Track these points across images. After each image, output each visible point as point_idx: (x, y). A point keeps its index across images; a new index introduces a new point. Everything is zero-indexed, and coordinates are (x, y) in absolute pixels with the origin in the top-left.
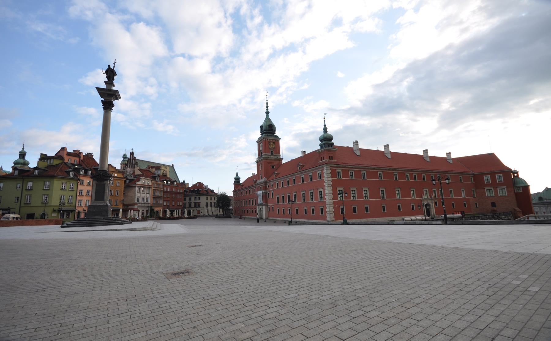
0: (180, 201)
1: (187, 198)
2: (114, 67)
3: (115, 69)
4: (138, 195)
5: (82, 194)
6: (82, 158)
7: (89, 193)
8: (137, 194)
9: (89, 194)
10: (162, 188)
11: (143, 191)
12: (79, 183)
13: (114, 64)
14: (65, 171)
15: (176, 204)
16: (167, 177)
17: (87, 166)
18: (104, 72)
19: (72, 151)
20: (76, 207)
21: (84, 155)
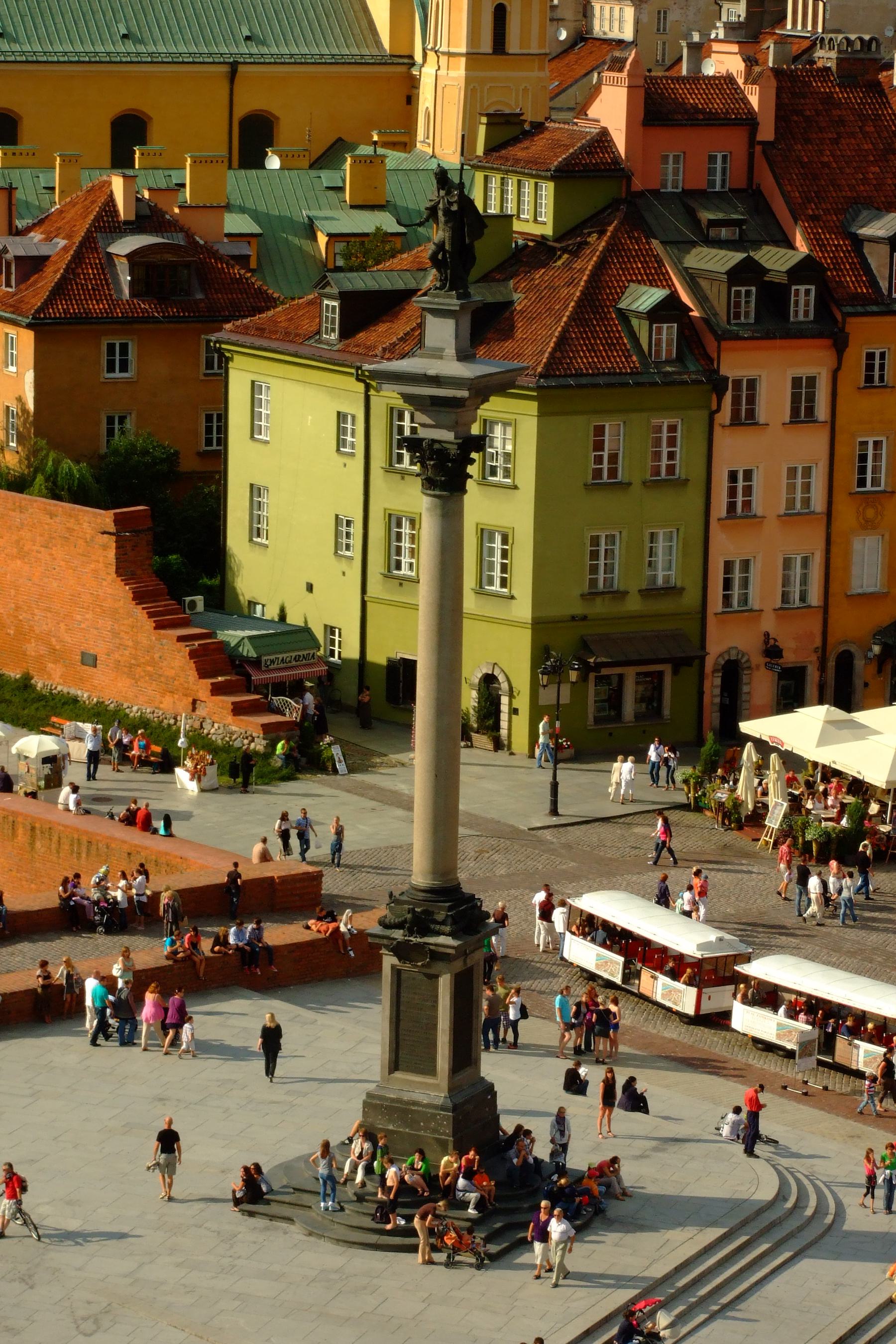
5: (747, 504)
6: (767, 132)
7: (807, 487)
9: (806, 502)
12: (725, 415)
20: (711, 621)
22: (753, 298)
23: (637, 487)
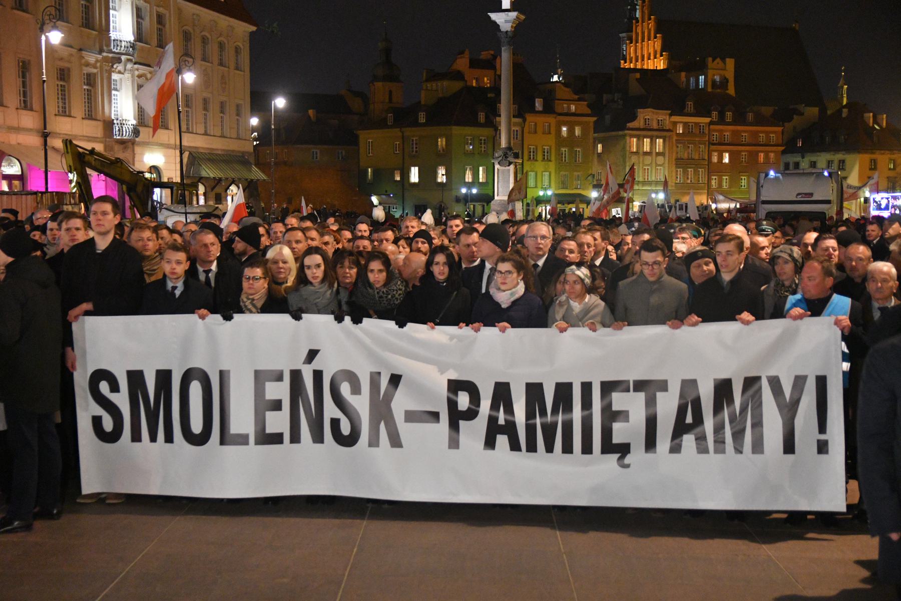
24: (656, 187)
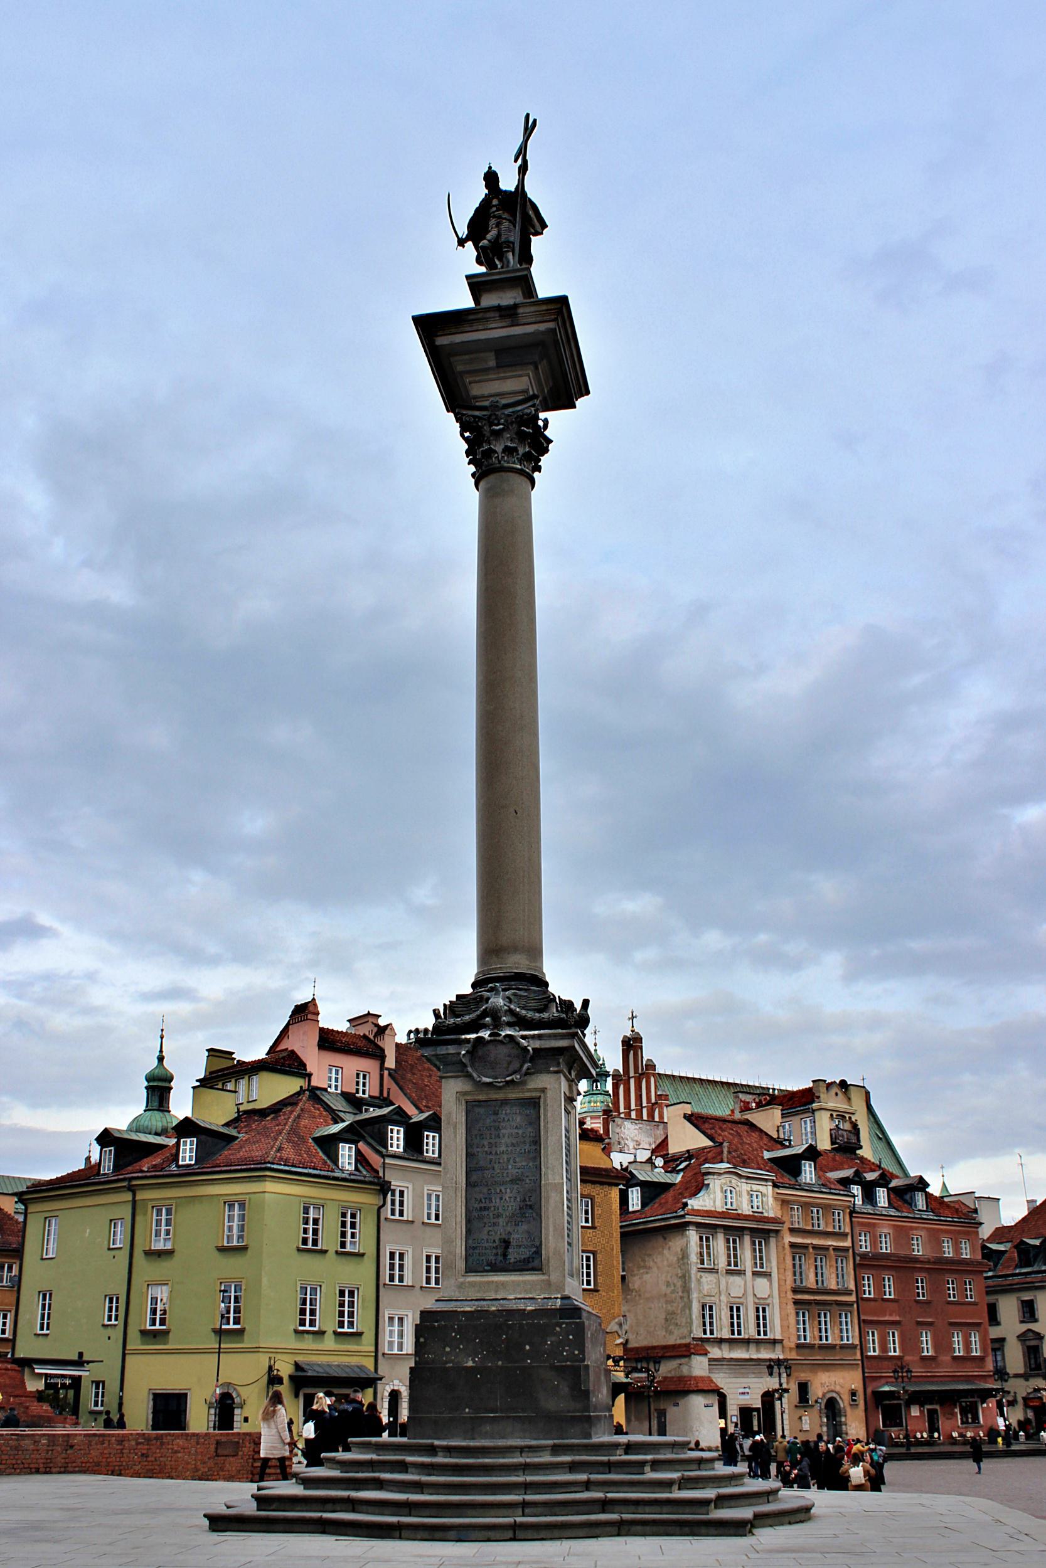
0: (966, 1327)
1: (1009, 1307)
2: (523, 169)
3: (533, 192)
4: (705, 1285)
6: (390, 1063)
8: (699, 1281)
10: (842, 1235)
11: (733, 1257)
12: (387, 1212)
13: (522, 151)
14: (315, 1139)
15: (942, 1344)
16: (863, 1159)
17: (417, 1107)
18: (463, 231)
19: (343, 1026)
21: (398, 1045)
22: (401, 1136)
23: (332, 1253)
24: (758, 1351)
